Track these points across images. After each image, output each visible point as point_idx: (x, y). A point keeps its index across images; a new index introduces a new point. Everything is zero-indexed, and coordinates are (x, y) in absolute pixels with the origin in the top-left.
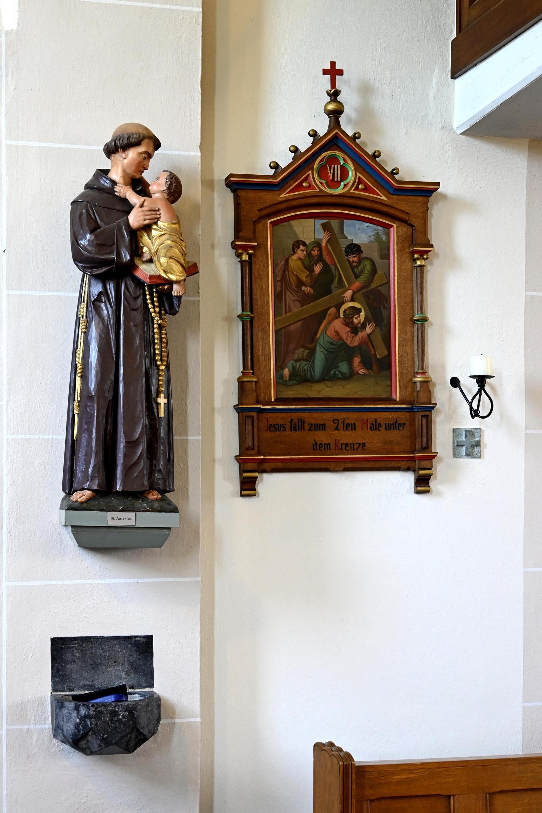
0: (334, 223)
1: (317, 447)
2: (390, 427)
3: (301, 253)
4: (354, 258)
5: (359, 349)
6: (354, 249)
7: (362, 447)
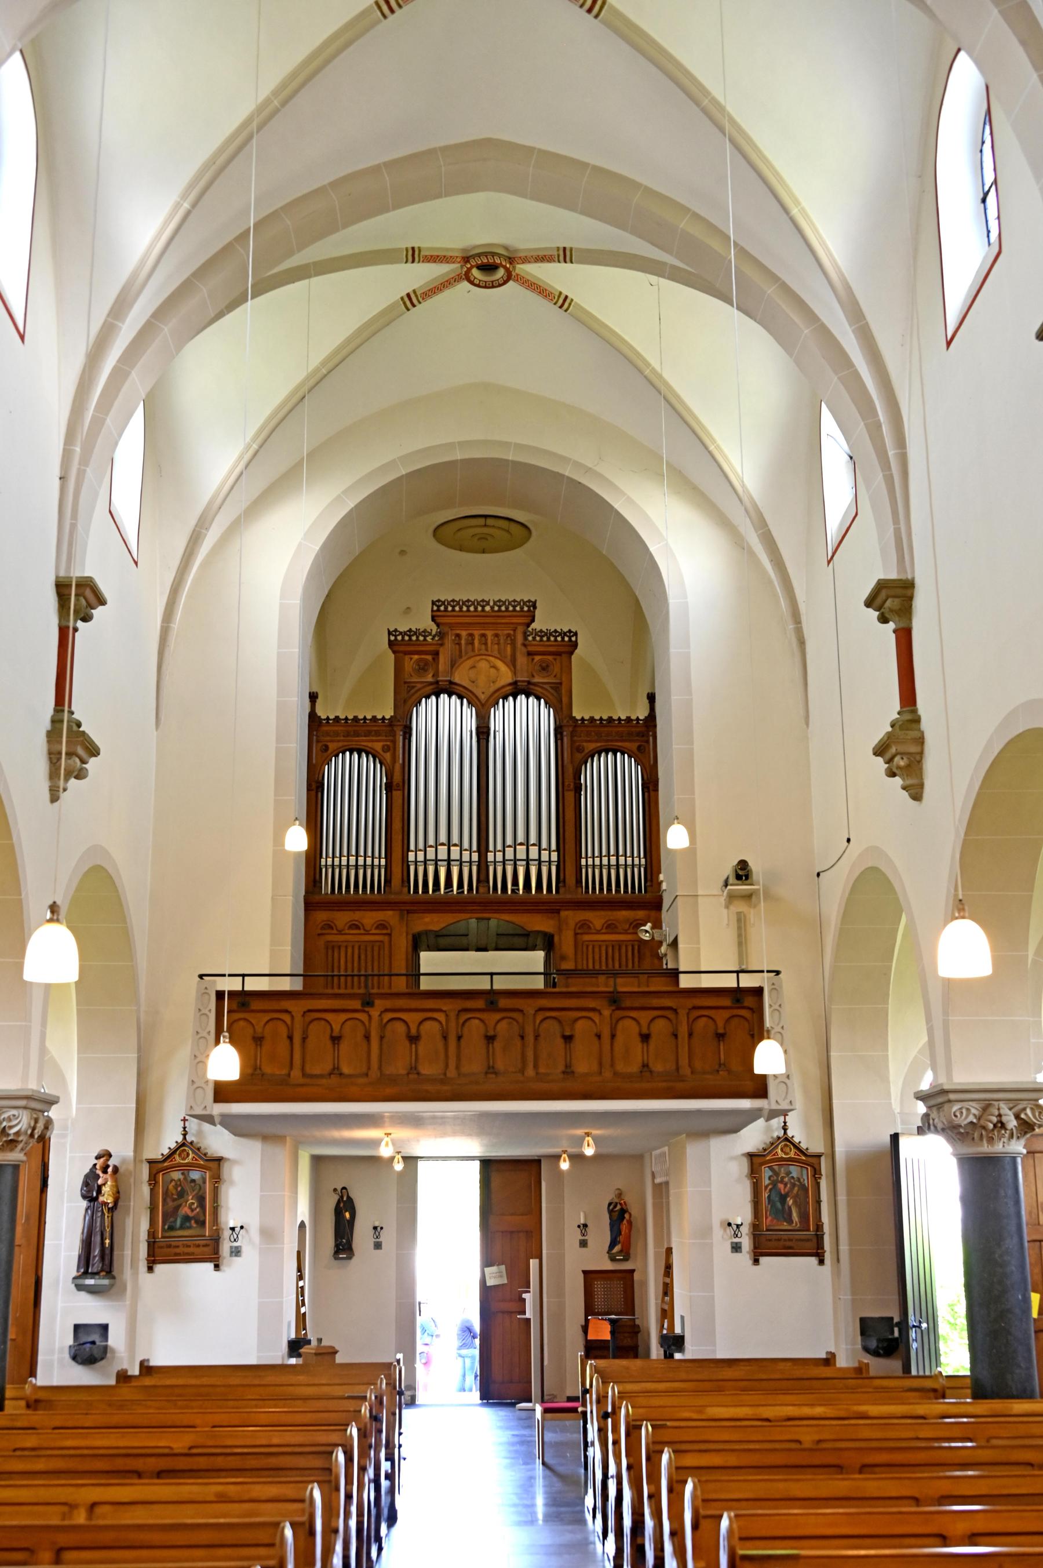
0: (186, 1172)
1: (176, 1254)
2: (204, 1246)
3: (173, 1183)
4: (193, 1184)
5: (193, 1218)
6: (193, 1181)
7: (193, 1254)
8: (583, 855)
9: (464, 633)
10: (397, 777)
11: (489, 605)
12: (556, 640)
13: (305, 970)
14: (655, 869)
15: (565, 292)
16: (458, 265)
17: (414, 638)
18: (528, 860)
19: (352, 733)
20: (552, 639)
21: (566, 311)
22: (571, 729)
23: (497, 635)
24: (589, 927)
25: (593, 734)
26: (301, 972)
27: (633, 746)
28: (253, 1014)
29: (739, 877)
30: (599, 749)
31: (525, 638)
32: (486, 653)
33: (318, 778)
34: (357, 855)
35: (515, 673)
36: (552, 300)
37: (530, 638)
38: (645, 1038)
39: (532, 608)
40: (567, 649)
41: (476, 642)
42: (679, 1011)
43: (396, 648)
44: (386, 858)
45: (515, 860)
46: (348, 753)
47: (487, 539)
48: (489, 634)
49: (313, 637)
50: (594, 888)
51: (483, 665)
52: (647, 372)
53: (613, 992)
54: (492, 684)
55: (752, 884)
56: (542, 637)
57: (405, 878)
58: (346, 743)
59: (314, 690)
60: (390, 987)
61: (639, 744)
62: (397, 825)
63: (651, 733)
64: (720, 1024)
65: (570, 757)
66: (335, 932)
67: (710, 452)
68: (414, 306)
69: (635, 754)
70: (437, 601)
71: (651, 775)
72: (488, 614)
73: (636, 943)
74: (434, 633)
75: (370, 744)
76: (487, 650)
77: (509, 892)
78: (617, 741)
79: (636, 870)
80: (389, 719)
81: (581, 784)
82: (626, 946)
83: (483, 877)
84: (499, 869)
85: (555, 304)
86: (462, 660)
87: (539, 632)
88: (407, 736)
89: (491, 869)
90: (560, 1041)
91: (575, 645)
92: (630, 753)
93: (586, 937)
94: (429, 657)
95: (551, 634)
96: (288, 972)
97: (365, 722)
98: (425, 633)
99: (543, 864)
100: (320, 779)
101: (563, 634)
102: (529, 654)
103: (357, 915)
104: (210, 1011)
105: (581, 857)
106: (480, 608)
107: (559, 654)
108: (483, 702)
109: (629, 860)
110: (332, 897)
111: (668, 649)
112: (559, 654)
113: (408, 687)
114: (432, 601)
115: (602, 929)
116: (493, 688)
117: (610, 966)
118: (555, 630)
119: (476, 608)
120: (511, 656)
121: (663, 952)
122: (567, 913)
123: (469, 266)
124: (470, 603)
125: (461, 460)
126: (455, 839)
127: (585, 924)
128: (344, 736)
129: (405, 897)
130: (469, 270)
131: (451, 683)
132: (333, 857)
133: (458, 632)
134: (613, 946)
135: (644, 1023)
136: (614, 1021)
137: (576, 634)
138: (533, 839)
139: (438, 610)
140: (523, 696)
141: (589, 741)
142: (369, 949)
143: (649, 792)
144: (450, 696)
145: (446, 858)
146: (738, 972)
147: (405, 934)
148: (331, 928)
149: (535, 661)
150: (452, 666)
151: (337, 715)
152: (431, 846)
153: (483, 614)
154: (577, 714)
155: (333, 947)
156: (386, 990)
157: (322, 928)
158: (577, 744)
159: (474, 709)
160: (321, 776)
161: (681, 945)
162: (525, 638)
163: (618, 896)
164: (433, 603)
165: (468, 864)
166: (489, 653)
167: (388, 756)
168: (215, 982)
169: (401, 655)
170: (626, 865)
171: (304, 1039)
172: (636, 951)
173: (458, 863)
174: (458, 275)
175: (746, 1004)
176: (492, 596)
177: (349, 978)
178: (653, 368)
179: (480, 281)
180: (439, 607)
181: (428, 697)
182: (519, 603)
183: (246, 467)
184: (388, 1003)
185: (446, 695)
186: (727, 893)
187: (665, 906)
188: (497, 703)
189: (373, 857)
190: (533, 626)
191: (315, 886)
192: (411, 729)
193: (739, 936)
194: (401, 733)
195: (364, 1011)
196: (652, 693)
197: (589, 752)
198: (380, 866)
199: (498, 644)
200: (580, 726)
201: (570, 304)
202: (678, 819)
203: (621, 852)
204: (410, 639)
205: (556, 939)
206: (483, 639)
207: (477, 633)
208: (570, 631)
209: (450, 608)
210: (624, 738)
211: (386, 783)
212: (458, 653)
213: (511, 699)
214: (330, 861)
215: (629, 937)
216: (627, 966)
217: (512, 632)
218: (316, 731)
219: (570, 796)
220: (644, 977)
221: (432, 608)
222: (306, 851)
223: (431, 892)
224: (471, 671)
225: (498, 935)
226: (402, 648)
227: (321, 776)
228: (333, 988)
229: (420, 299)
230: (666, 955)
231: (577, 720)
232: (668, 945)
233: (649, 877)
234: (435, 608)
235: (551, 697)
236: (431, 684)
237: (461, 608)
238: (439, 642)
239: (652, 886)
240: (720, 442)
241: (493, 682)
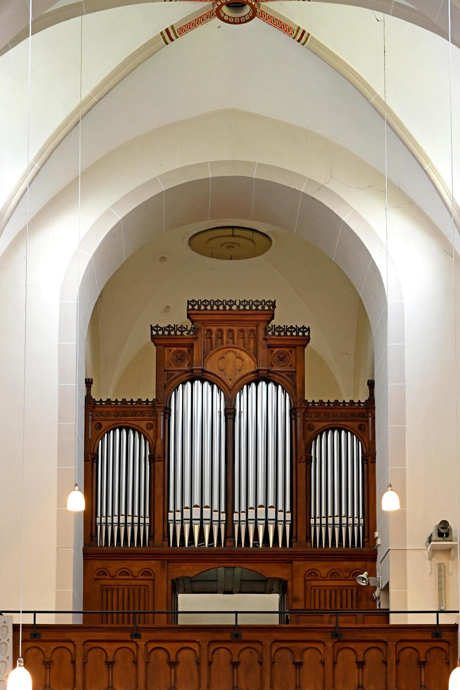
8: (312, 516)
9: (214, 329)
10: (159, 450)
11: (236, 304)
12: (292, 335)
13: (84, 608)
14: (371, 528)
15: (303, 28)
16: (210, 3)
17: (173, 333)
18: (266, 520)
19: (121, 413)
20: (289, 334)
21: (303, 44)
22: (303, 411)
23: (242, 331)
24: (317, 576)
25: (322, 414)
26: (82, 610)
27: (355, 425)
28: (43, 643)
29: (440, 535)
30: (326, 427)
31: (266, 334)
32: (233, 346)
33: (93, 451)
34: (126, 515)
35: (257, 363)
36: (291, 34)
37: (270, 333)
38: (361, 665)
39: (271, 307)
40: (301, 343)
41: (225, 336)
42: (388, 643)
43: (157, 342)
44: (150, 517)
45: (256, 520)
46: (118, 431)
47: (234, 247)
48: (236, 329)
49: (87, 334)
50: (321, 543)
51: (230, 356)
52: (373, 100)
53: (335, 628)
54: (238, 372)
55: (451, 541)
56: (280, 332)
57: (166, 535)
58: (117, 422)
59: (89, 377)
60: (154, 623)
61: (360, 423)
62: (159, 490)
63: (370, 414)
64: (422, 653)
65: (302, 435)
66: (108, 577)
67: (425, 171)
68: (172, 40)
69: (356, 432)
70: (192, 301)
71: (369, 449)
72: (235, 312)
73: (355, 588)
74: (189, 328)
75: (136, 423)
76: (233, 343)
77: (251, 546)
78: (341, 421)
79: (356, 528)
80: (152, 402)
81: (312, 457)
82: (347, 590)
83: (229, 533)
84: (243, 527)
85: (294, 38)
86: (212, 352)
87: (277, 328)
88: (167, 416)
89: (236, 527)
90: (291, 667)
91: (308, 339)
92: (353, 431)
93: (314, 583)
94: (185, 349)
95: (287, 330)
96: (71, 610)
97: (132, 404)
98: (182, 328)
99: (279, 523)
100: (95, 451)
101: (298, 330)
102: (269, 346)
103: (126, 564)
104: (8, 640)
105: (310, 518)
106: (228, 308)
107: (294, 347)
108: (230, 388)
109: (350, 521)
110: (106, 549)
111: (385, 342)
112: (294, 347)
113: (167, 374)
114: (188, 301)
115: (327, 576)
116: (239, 376)
117: (333, 607)
118: (291, 326)
119: (224, 307)
120: (254, 349)
121: (376, 595)
122: (298, 563)
123: (219, 3)
124: (220, 303)
125: (212, 178)
126: (207, 502)
127: (312, 572)
128: (114, 416)
129: (166, 550)
130: (220, 7)
131: (203, 371)
132: (107, 516)
133: (210, 328)
134: (336, 590)
135: (360, 653)
136: (336, 651)
137: (308, 330)
138: (271, 502)
139: (193, 309)
140: (264, 383)
141: (319, 421)
142: (136, 592)
143: (367, 464)
144: (202, 383)
145: (199, 517)
146: (437, 612)
147: (165, 580)
148: (105, 574)
149: (274, 352)
150: (204, 359)
151: (109, 398)
152: (187, 508)
153: (231, 312)
154: (309, 398)
155: (107, 590)
156: (151, 625)
157: (98, 574)
158: (309, 423)
159: (222, 393)
160: (96, 448)
161: (392, 590)
162: (266, 334)
163: (341, 549)
164: (189, 303)
165: (217, 523)
166: (236, 346)
167: (151, 433)
168: (12, 617)
169: (162, 347)
170: (347, 524)
171: (84, 664)
172: (355, 594)
173: (209, 522)
174: (210, 12)
175: (444, 638)
176: (238, 297)
177: (120, 615)
178: (378, 96)
179: (229, 17)
180: (193, 306)
181: (184, 383)
182: (261, 303)
183: (30, 184)
184: (153, 636)
185: (199, 382)
186: (431, 548)
187: (379, 558)
188: (242, 389)
189: (139, 517)
190: (273, 322)
191: (91, 540)
192: (170, 410)
193: (440, 583)
194: (162, 413)
195: (133, 642)
196: (371, 381)
197: (319, 429)
198: (145, 523)
199: (243, 338)
200: (311, 408)
201: (307, 38)
202: (391, 486)
203: (343, 513)
204: (169, 334)
205: (289, 584)
206: (230, 333)
207: (225, 329)
208: (303, 327)
209: (203, 308)
210: (348, 418)
211: (149, 455)
212: (209, 345)
213: (253, 385)
214: (104, 520)
215: (350, 583)
216: (347, 606)
217: (255, 328)
218: (92, 411)
219: (302, 466)
220: (360, 616)
221: (188, 307)
222: (84, 511)
223: (187, 546)
224: (220, 361)
225: (241, 580)
226: (163, 342)
227: (96, 448)
228: (107, 623)
229: (178, 34)
230: (379, 598)
231: (309, 403)
232: (381, 590)
233: (366, 534)
234: (190, 307)
235: (287, 384)
236: (187, 372)
237: (212, 307)
238: (194, 336)
239: (368, 541)
240: (434, 162)
241: (239, 371)
